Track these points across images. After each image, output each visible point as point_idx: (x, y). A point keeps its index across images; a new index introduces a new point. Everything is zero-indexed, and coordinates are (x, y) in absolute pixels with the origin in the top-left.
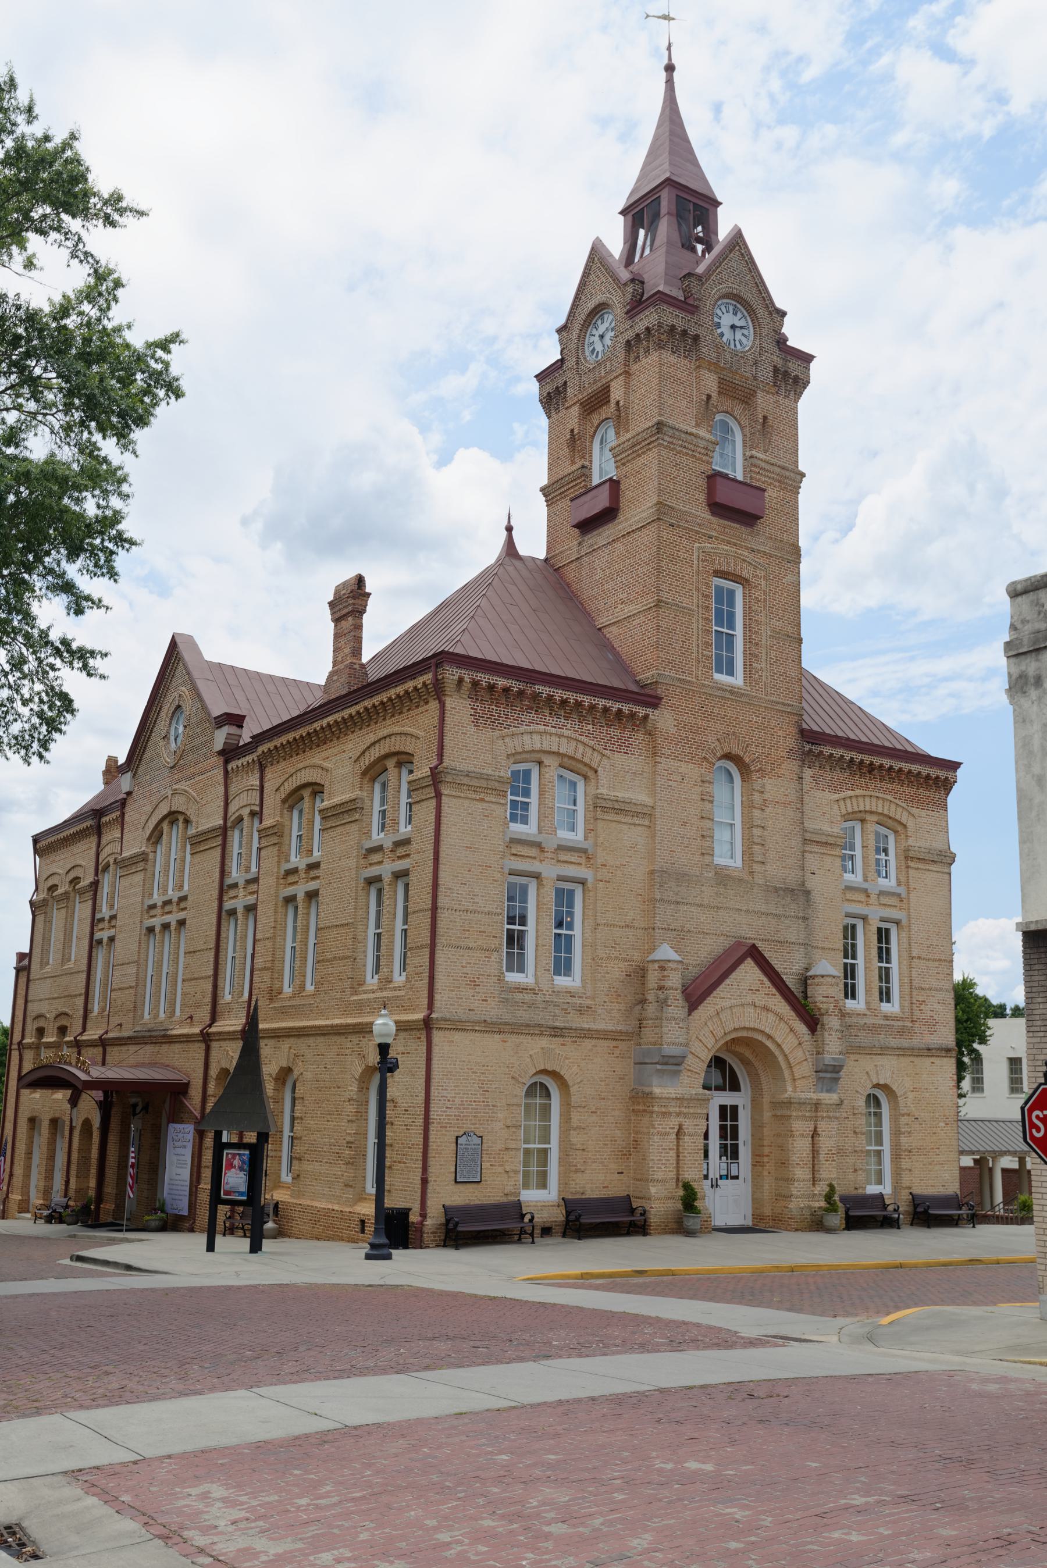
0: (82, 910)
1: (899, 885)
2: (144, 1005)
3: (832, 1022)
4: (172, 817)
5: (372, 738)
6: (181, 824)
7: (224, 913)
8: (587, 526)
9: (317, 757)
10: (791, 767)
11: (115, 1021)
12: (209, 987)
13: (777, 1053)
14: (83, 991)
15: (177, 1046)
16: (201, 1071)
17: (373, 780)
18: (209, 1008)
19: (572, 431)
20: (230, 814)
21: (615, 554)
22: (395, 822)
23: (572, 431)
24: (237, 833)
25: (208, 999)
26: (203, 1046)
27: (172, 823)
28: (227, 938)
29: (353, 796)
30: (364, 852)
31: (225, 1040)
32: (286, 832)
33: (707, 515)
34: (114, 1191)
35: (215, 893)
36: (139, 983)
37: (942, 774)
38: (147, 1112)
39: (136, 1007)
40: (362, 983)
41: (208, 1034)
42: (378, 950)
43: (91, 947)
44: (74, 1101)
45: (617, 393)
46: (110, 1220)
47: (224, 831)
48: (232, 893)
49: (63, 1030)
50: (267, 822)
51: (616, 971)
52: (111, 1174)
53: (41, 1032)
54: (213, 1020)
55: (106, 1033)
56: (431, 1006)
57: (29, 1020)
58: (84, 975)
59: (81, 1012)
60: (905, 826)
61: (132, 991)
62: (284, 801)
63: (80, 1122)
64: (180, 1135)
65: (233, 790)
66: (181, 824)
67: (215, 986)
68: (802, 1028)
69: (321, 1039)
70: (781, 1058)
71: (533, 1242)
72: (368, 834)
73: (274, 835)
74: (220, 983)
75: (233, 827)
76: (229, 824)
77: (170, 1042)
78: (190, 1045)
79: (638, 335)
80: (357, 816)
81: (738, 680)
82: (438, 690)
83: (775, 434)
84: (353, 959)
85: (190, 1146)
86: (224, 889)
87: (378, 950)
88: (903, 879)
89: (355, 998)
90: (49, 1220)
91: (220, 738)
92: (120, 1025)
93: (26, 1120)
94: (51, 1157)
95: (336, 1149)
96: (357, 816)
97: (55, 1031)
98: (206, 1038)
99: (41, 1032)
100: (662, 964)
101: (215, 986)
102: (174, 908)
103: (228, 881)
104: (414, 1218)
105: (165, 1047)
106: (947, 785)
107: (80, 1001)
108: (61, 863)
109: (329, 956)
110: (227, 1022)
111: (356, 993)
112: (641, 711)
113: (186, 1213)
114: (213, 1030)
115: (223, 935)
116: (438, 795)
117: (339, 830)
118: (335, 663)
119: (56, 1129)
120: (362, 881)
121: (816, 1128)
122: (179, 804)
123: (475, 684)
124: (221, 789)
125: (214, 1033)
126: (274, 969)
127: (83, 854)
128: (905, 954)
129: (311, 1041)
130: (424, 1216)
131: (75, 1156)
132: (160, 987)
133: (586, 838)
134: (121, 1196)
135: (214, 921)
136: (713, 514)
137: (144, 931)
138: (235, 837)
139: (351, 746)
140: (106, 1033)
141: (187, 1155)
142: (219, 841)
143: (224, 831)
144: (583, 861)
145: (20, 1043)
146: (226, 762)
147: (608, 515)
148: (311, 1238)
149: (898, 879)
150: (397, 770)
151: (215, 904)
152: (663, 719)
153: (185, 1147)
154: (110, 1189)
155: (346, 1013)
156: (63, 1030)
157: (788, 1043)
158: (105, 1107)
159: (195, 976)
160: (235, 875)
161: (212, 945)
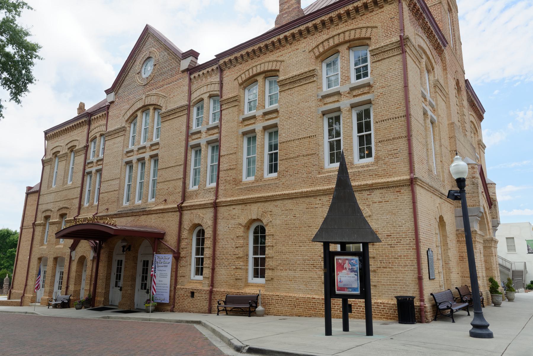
0: (80, 159)
2: (123, 199)
4: (145, 109)
5: (325, 37)
6: (151, 111)
7: (189, 147)
9: (272, 57)
11: (102, 208)
12: (180, 183)
14: (79, 196)
15: (153, 215)
17: (322, 61)
18: (180, 194)
20: (192, 100)
22: (348, 78)
24: (194, 110)
25: (180, 189)
26: (178, 214)
27: (143, 112)
28: (191, 159)
29: (311, 69)
30: (320, 97)
31: (196, 209)
32: (242, 99)
34: (104, 291)
35: (184, 137)
36: (121, 188)
38: (130, 250)
39: (119, 200)
40: (322, 168)
41: (181, 207)
43: (84, 176)
44: (73, 247)
46: (101, 306)
47: (188, 107)
48: (194, 137)
49: (63, 216)
50: (224, 97)
52: (101, 283)
53: (47, 218)
54: (184, 199)
55: (97, 214)
56: (412, 170)
57: (39, 213)
58: (80, 189)
59: (77, 206)
61: (116, 192)
62: (240, 85)
63: (77, 258)
64: (162, 260)
65: (194, 87)
66: (151, 111)
67: (184, 183)
69: (290, 201)
71: (469, 315)
72: (321, 88)
73: (236, 101)
74: (187, 182)
75: (193, 106)
76: (192, 104)
77: (148, 214)
78: (165, 214)
80: (315, 79)
84: (315, 154)
85: (170, 266)
86: (188, 135)
89: (320, 176)
90: (55, 306)
91: (185, 64)
92: (107, 209)
93: (37, 259)
94: (54, 276)
95: (311, 262)
96: (315, 79)
97: (58, 216)
98: (180, 209)
99: (47, 218)
100: (473, 165)
101: (184, 183)
102: (148, 149)
103: (191, 131)
104: (417, 303)
105: (143, 218)
107: (77, 202)
108: (62, 142)
109: (292, 156)
110: (191, 201)
111: (319, 173)
113: (167, 301)
114: (183, 205)
115: (188, 158)
116: (404, 52)
117: (297, 89)
118: (280, 11)
119: (56, 262)
120: (320, 113)
122: (153, 100)
124: (187, 88)
125: (187, 206)
126: (235, 168)
127: (79, 137)
129: (278, 203)
130: (422, 300)
131: (73, 274)
132: (136, 189)
134: (107, 294)
135: (183, 150)
137: (124, 163)
138: (194, 110)
140: (97, 214)
141: (168, 271)
142: (186, 112)
143: (188, 107)
145: (34, 224)
146: (190, 74)
148: (292, 315)
150: (348, 51)
151: (184, 143)
153: (166, 266)
154: (99, 290)
155: (312, 184)
156: (63, 216)
158: (97, 250)
159: (168, 180)
160: (194, 128)
161: (182, 162)
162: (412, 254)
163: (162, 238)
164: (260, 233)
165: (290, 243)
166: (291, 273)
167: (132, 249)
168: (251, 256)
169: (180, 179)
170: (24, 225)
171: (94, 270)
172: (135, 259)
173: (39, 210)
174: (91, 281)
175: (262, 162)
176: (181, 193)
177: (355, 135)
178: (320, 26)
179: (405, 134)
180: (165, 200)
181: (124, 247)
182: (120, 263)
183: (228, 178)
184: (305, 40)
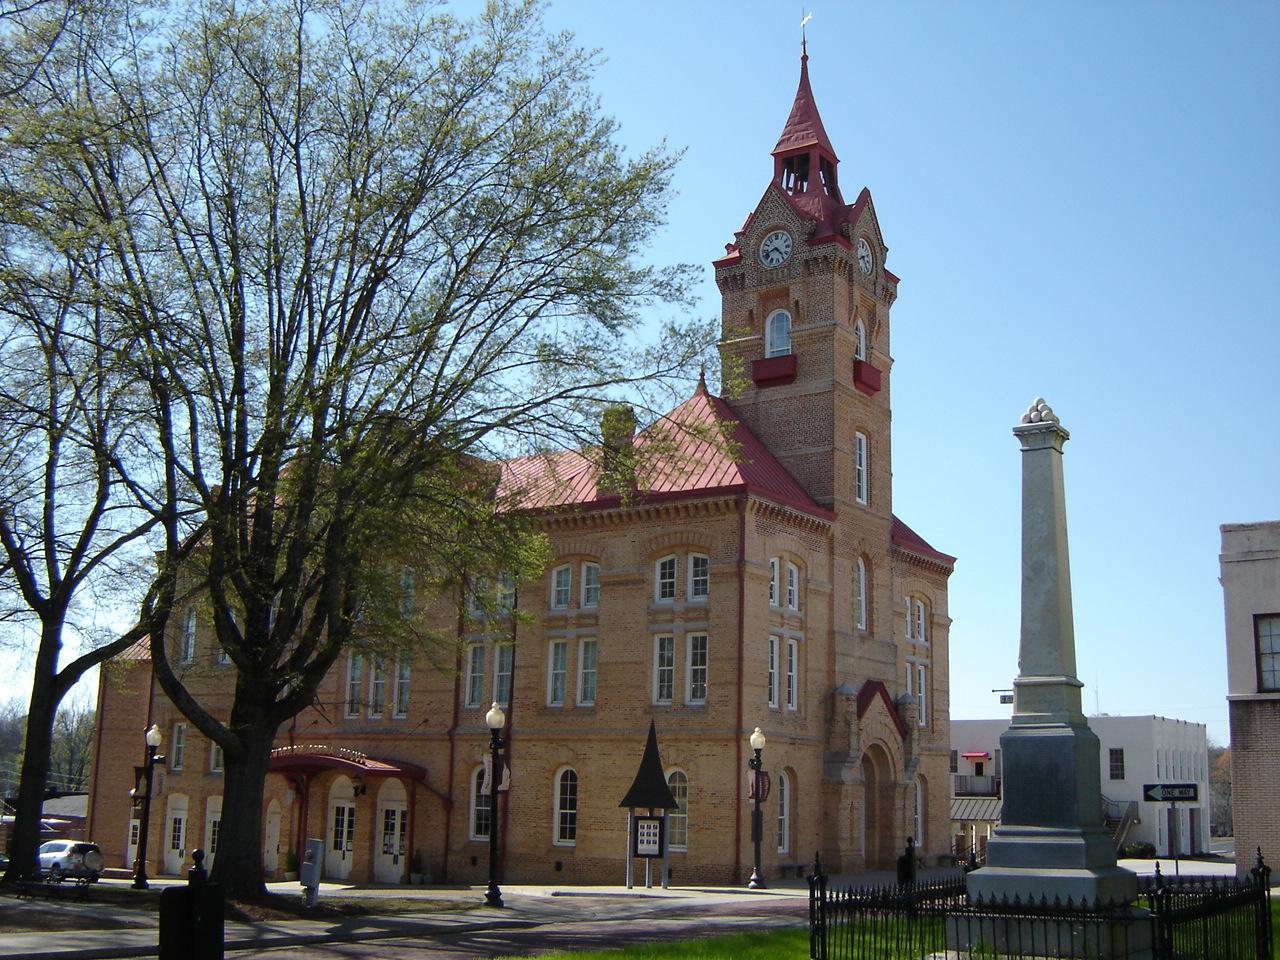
1: (926, 640)
3: (916, 734)
8: (762, 382)
10: (887, 560)
12: (451, 698)
13: (888, 753)
16: (445, 765)
19: (751, 312)
21: (793, 407)
23: (751, 312)
25: (451, 707)
26: (449, 744)
33: (853, 388)
37: (948, 566)
38: (364, 794)
42: (770, 689)
45: (796, 294)
51: (814, 702)
60: (931, 602)
67: (457, 697)
68: (899, 738)
70: (889, 758)
79: (816, 259)
81: (863, 501)
82: (739, 506)
83: (877, 326)
87: (770, 689)
88: (929, 637)
101: (457, 697)
106: (948, 571)
112: (828, 523)
121: (904, 805)
123: (761, 505)
128: (929, 687)
133: (800, 610)
136: (856, 387)
139: (633, 532)
144: (798, 625)
147: (788, 378)
149: (926, 636)
152: (836, 529)
157: (894, 747)
162: (733, 814)
163: (423, 778)
164: (570, 783)
165: (607, 796)
166: (607, 834)
167: (368, 791)
168: (557, 811)
169: (451, 691)
170: (105, 725)
171: (296, 822)
172: (374, 807)
173: (154, 705)
174: (291, 839)
175: (575, 684)
176: (452, 712)
177: (689, 667)
178: (653, 514)
179: (736, 680)
180: (426, 721)
181: (356, 789)
182: (340, 811)
183: (526, 702)
184: (634, 526)
